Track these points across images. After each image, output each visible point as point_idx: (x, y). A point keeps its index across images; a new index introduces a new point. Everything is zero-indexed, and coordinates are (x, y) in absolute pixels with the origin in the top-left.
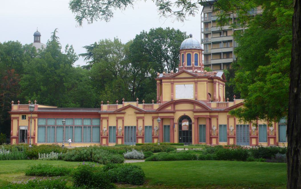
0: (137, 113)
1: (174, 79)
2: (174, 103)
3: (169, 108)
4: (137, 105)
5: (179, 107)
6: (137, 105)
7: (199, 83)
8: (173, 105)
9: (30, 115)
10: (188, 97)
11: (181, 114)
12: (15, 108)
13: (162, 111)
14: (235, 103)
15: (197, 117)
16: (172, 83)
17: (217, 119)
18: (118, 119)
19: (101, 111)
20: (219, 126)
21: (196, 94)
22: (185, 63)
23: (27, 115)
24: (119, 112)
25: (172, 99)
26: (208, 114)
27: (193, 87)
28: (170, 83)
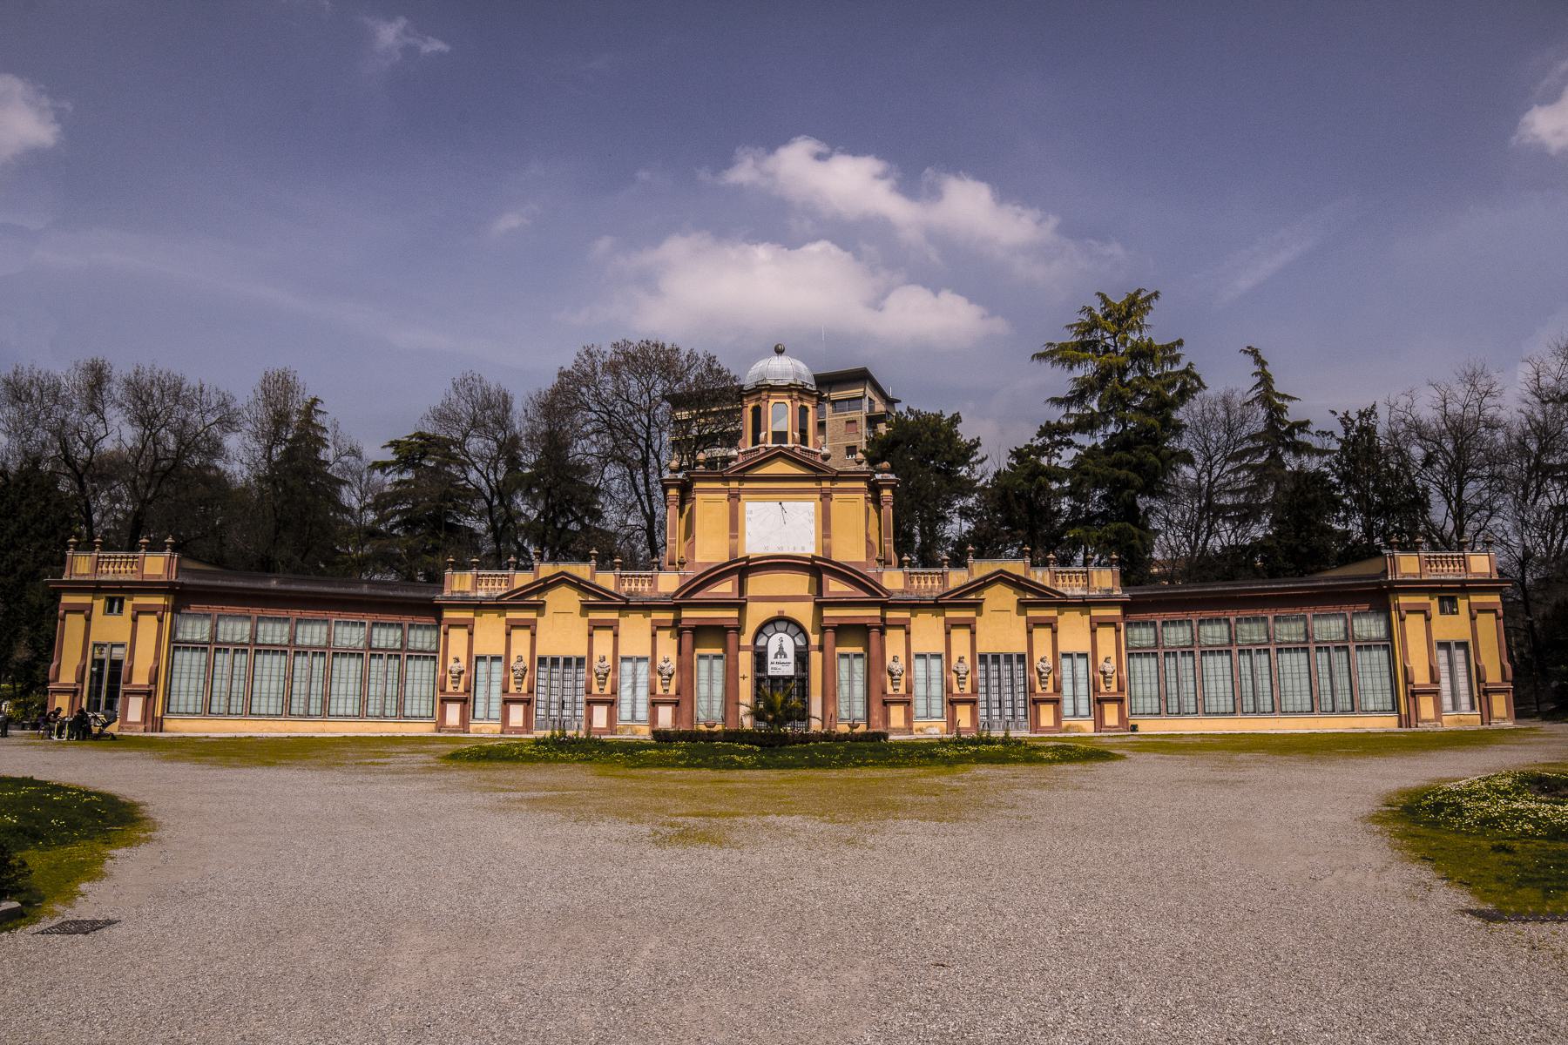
1: (742, 480)
2: (743, 569)
3: (726, 588)
4: (593, 576)
5: (758, 584)
6: (593, 576)
9: (140, 600)
11: (771, 610)
13: (700, 596)
14: (971, 574)
15: (836, 622)
16: (734, 497)
17: (908, 633)
19: (447, 593)
22: (766, 435)
25: (733, 553)
26: (877, 612)
28: (725, 496)
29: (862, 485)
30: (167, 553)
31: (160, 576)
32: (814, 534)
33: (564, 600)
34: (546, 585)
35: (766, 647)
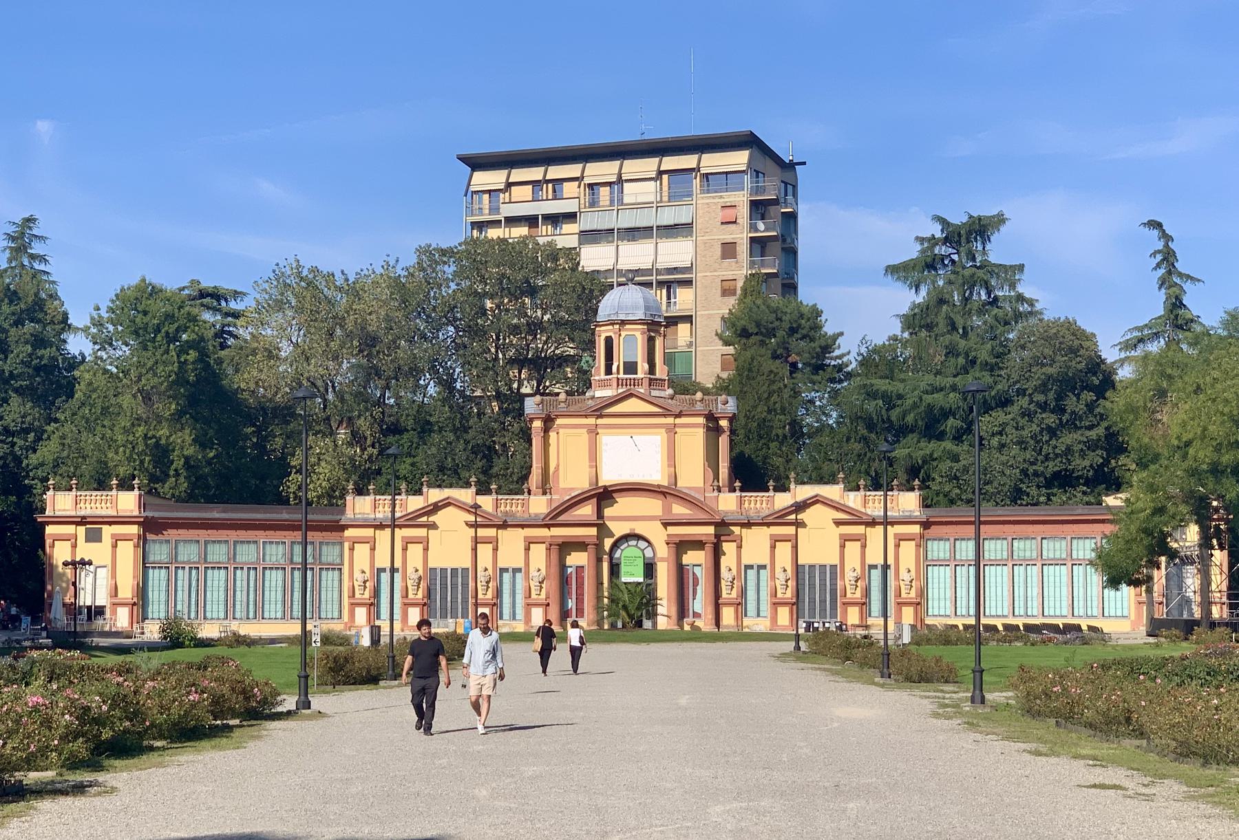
0: (838, 523)
2: (604, 496)
3: (587, 511)
12: (60, 502)
13: (563, 518)
15: (677, 540)
16: (594, 432)
18: (775, 540)
23: (105, 528)
24: (779, 519)
26: (711, 530)
27: (659, 443)
30: (136, 492)
31: (132, 511)
32: (660, 462)
33: (450, 519)
34: (436, 508)
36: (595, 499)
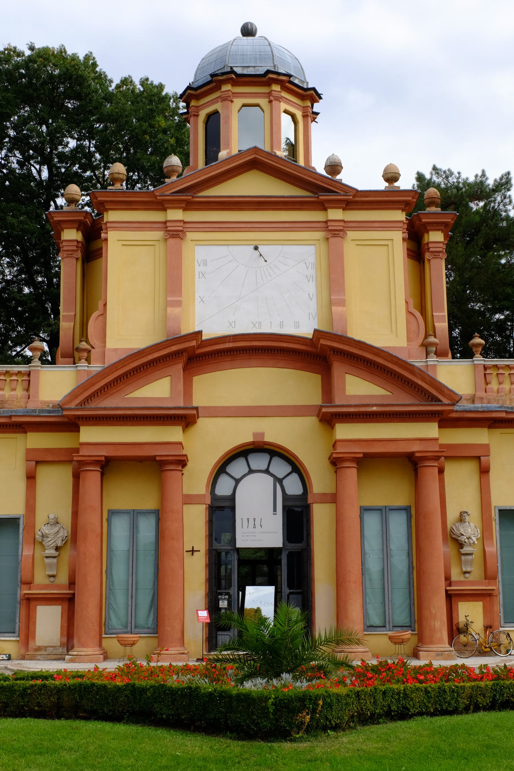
7: (351, 234)
8: (178, 368)
10: (281, 325)
15: (359, 450)
20: (495, 515)
21: (331, 303)
27: (312, 259)
28: (158, 235)
29: (400, 216)
35: (232, 498)
36: (179, 367)
